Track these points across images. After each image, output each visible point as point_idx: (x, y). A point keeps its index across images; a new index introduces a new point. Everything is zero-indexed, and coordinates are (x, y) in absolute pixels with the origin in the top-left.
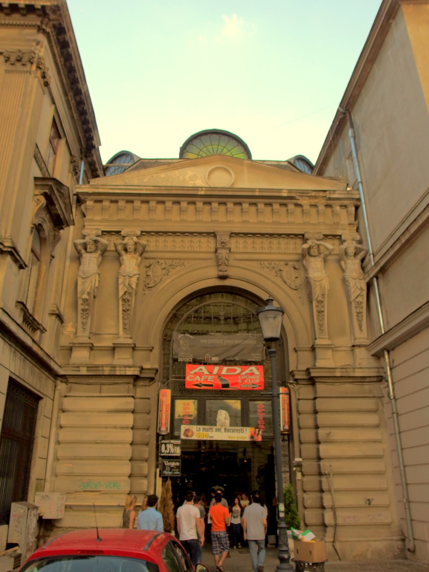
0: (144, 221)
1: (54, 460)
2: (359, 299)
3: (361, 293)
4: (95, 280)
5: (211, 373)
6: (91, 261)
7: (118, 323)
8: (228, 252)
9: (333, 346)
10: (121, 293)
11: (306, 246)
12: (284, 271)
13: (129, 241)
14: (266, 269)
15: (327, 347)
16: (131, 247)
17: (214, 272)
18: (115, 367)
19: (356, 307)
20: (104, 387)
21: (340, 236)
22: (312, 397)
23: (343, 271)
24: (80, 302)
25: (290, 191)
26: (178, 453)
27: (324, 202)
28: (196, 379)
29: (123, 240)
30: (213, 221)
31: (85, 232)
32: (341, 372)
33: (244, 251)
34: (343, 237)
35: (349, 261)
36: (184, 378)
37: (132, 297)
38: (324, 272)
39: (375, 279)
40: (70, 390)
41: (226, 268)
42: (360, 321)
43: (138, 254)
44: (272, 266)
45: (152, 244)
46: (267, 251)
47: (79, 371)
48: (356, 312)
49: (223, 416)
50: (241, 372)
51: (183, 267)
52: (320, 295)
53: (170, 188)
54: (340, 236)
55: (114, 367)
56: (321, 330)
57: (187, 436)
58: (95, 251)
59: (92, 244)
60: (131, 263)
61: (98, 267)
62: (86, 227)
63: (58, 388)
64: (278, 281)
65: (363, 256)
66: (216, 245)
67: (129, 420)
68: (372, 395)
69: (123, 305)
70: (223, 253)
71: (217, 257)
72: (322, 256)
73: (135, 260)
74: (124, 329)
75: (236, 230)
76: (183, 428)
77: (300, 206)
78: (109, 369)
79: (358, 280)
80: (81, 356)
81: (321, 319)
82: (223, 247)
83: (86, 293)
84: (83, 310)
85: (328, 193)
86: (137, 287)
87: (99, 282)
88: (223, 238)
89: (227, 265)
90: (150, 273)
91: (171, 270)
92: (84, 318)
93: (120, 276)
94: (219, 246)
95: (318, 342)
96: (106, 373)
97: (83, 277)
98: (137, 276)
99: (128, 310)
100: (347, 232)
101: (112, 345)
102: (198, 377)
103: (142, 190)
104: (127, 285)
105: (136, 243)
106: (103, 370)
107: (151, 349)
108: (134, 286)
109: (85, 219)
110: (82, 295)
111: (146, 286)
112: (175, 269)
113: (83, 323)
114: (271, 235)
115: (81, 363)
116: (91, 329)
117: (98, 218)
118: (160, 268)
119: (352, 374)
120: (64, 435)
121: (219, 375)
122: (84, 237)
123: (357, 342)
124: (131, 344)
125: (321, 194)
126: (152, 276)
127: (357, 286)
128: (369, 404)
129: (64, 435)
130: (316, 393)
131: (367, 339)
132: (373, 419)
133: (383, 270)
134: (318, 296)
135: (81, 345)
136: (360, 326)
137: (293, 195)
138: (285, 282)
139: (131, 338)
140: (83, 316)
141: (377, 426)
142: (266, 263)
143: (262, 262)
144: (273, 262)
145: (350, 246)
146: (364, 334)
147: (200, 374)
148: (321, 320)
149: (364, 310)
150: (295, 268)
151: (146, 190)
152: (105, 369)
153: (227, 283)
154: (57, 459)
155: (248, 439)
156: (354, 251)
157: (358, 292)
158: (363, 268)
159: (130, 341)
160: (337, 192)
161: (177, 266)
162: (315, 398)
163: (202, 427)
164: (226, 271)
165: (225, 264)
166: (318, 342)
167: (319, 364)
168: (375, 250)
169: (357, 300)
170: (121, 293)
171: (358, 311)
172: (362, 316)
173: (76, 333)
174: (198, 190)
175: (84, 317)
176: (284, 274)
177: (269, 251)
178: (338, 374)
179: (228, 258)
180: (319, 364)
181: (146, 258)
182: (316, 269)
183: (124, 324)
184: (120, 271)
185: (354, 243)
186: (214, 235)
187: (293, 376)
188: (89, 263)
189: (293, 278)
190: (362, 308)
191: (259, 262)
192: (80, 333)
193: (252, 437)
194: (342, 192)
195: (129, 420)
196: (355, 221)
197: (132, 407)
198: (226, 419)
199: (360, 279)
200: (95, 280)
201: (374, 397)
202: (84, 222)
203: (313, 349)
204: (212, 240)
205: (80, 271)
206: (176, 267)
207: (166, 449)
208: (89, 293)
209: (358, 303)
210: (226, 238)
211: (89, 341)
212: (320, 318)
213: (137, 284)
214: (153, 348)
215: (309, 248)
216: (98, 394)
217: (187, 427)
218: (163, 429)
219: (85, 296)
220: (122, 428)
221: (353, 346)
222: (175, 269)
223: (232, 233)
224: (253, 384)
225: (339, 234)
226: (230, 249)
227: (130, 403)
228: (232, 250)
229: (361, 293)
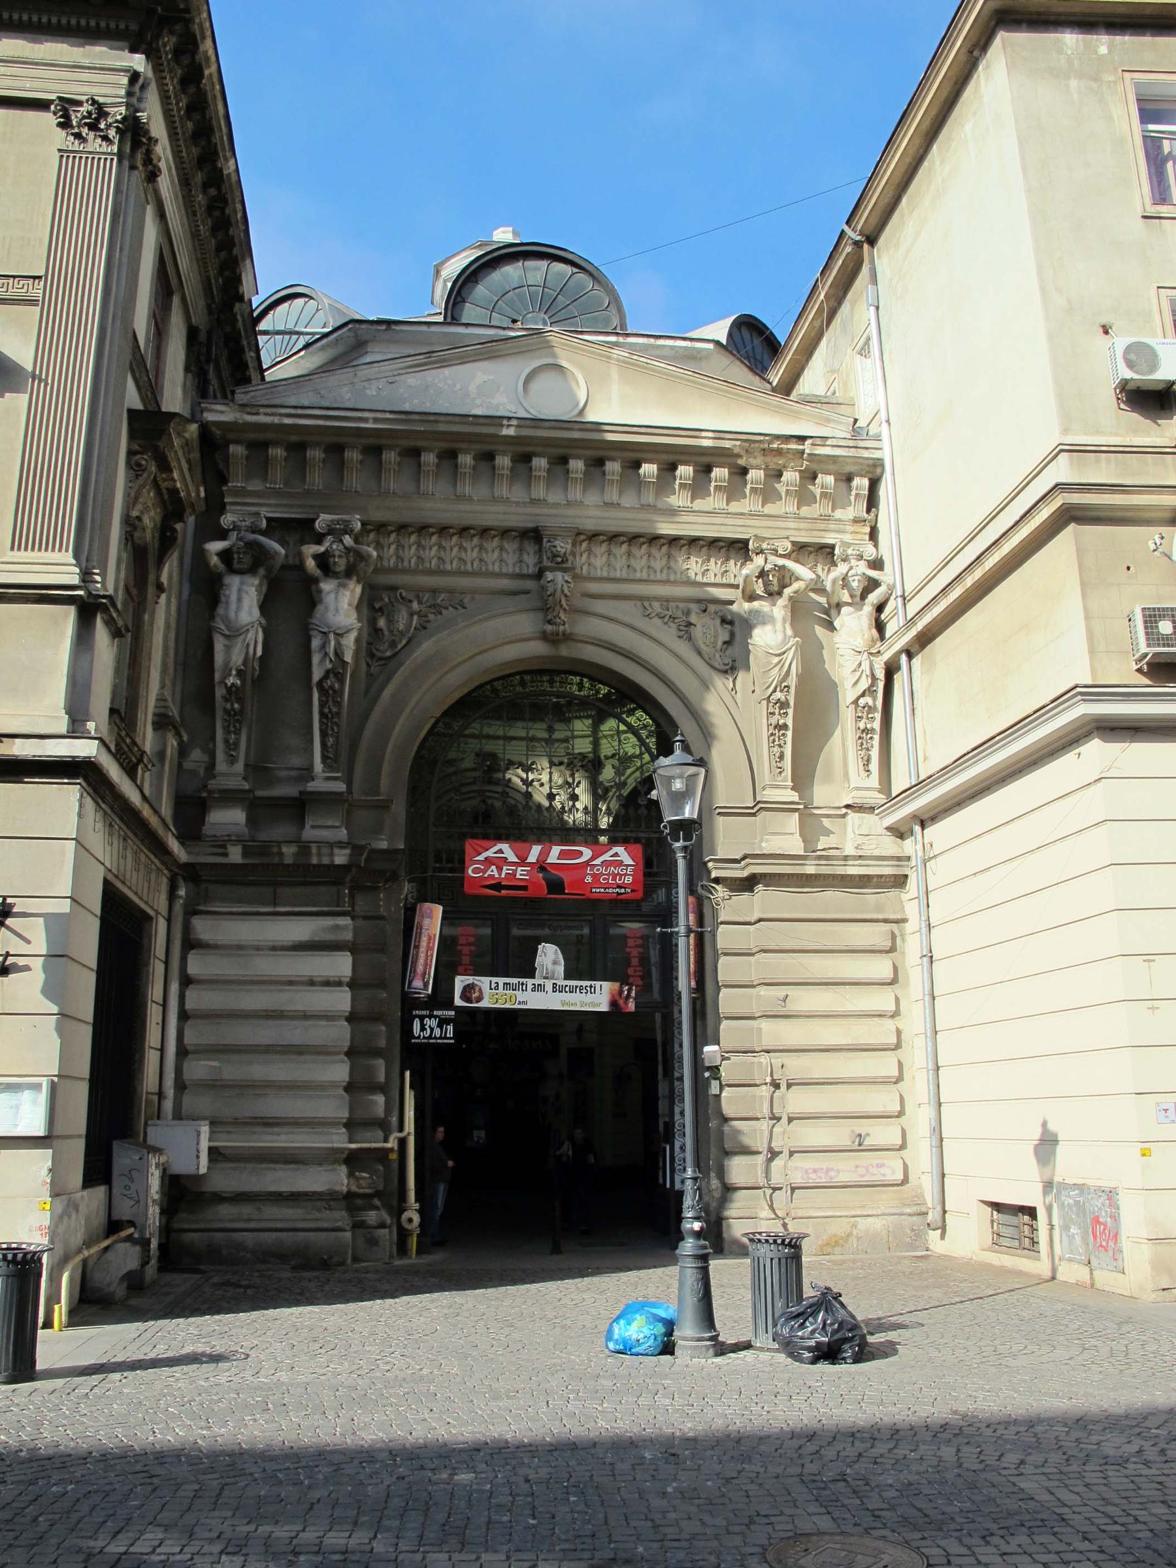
2: (868, 700)
3: (872, 685)
5: (523, 861)
10: (317, 675)
12: (699, 627)
14: (656, 621)
20: (284, 891)
24: (220, 692)
25: (719, 434)
26: (450, 1038)
28: (489, 872)
36: (463, 869)
37: (342, 682)
39: (904, 658)
44: (670, 613)
46: (659, 577)
49: (549, 956)
50: (593, 858)
53: (432, 418)
54: (833, 547)
57: (469, 1000)
62: (228, 507)
63: (182, 892)
64: (683, 648)
71: (543, 588)
73: (348, 593)
74: (324, 758)
75: (590, 525)
76: (460, 982)
83: (234, 672)
85: (808, 442)
90: (382, 623)
93: (313, 633)
94: (546, 563)
96: (288, 860)
97: (227, 633)
102: (493, 867)
103: (365, 420)
104: (332, 655)
109: (225, 488)
112: (441, 613)
113: (226, 741)
119: (840, 871)
120: (196, 999)
121: (541, 866)
125: (793, 446)
126: (386, 633)
128: (874, 935)
129: (196, 999)
132: (881, 968)
133: (925, 639)
137: (727, 444)
138: (700, 653)
140: (229, 726)
144: (672, 604)
146: (874, 781)
147: (501, 862)
151: (376, 420)
152: (284, 849)
153: (564, 651)
154: (183, 1052)
155: (604, 1007)
157: (864, 684)
158: (880, 627)
159: (341, 787)
161: (446, 608)
163: (502, 981)
168: (909, 589)
169: (862, 702)
170: (317, 675)
171: (862, 725)
174: (502, 426)
176: (697, 632)
177: (664, 576)
183: (324, 744)
184: (314, 621)
185: (862, 564)
189: (720, 643)
191: (639, 603)
192: (221, 766)
193: (614, 1003)
196: (868, 511)
197: (348, 936)
198: (555, 963)
199: (871, 654)
200: (256, 642)
204: (530, 548)
205: (218, 619)
206: (444, 611)
207: (423, 1029)
208: (240, 673)
210: (563, 546)
216: (271, 909)
217: (470, 979)
218: (418, 983)
220: (327, 983)
224: (619, 887)
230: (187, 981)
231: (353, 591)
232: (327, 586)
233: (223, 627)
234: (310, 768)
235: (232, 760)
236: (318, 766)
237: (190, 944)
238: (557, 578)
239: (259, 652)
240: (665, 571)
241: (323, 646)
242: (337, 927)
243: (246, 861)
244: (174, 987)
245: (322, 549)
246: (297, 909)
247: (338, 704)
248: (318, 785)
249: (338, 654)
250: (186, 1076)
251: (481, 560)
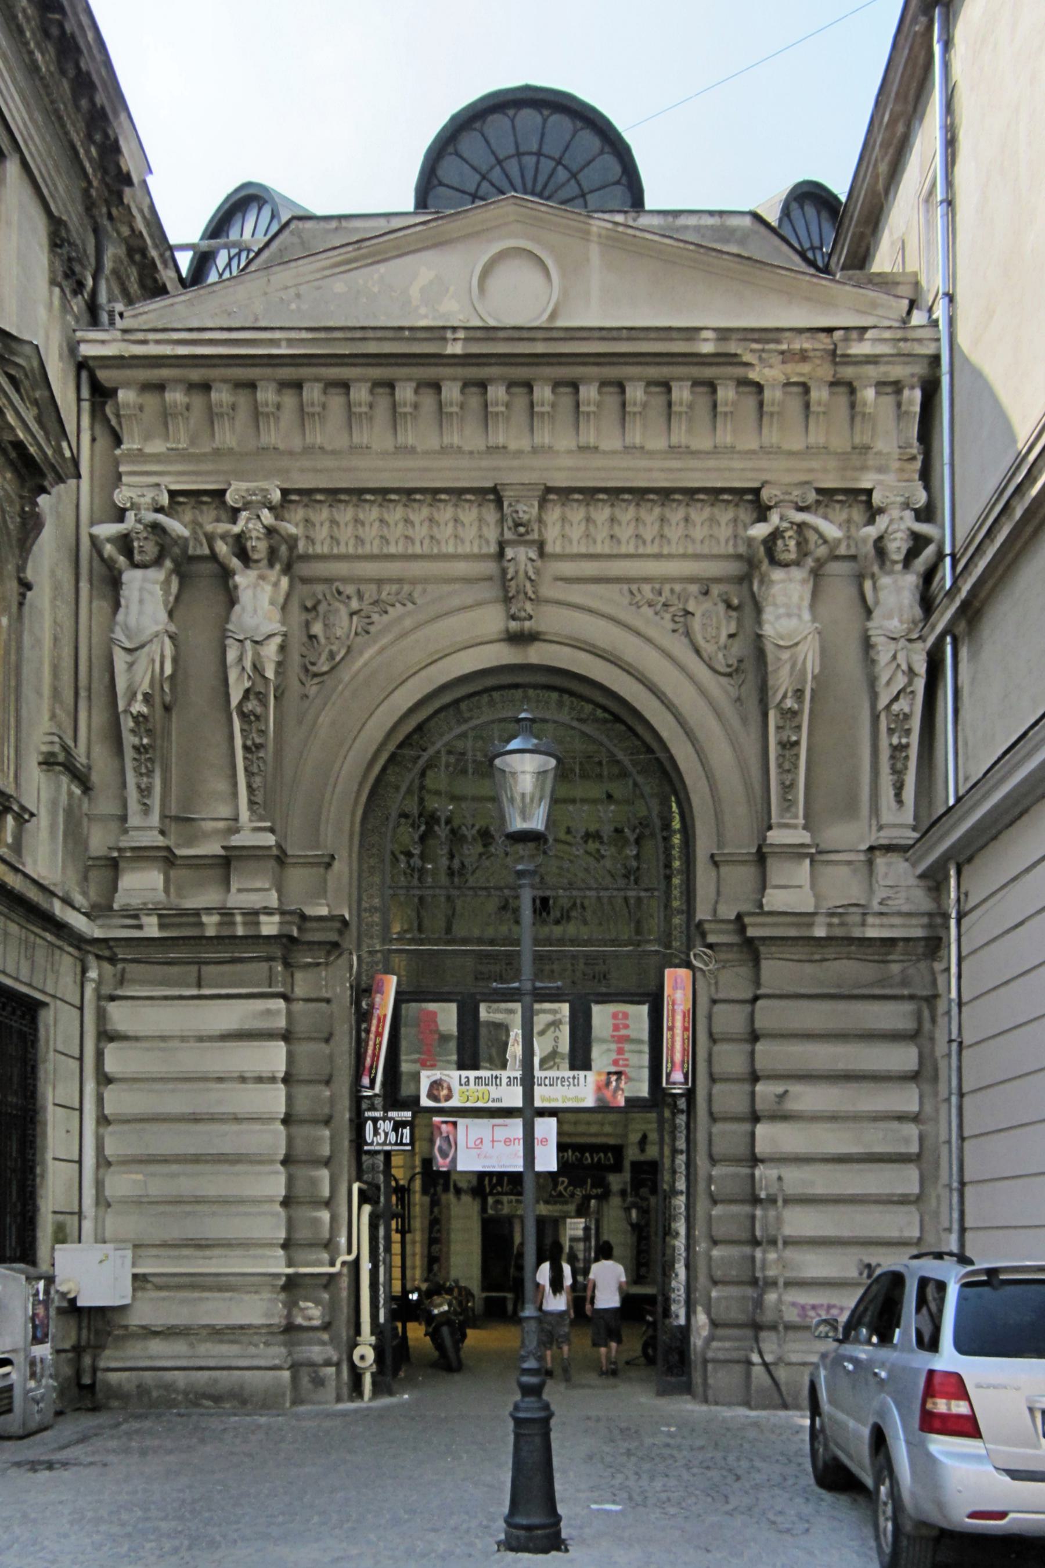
0: (291, 453)
1: (98, 1166)
4: (162, 657)
6: (147, 594)
7: (235, 785)
8: (533, 555)
9: (813, 851)
10: (234, 701)
11: (760, 531)
12: (698, 615)
13: (250, 526)
15: (795, 853)
16: (259, 547)
17: (492, 620)
18: (232, 914)
19: (891, 731)
20: (208, 970)
21: (869, 492)
22: (749, 995)
23: (869, 612)
27: (826, 372)
29: (234, 521)
30: (493, 450)
31: (121, 496)
32: (830, 925)
33: (583, 550)
34: (877, 499)
35: (885, 581)
37: (265, 705)
38: (807, 616)
40: (122, 980)
41: (529, 607)
42: (898, 773)
43: (278, 567)
45: (319, 531)
47: (140, 927)
48: (891, 745)
51: (410, 606)
52: (790, 694)
54: (869, 492)
55: (226, 914)
56: (786, 800)
58: (158, 562)
59: (146, 538)
60: (260, 601)
61: (171, 614)
62: (125, 479)
63: (93, 974)
65: (932, 560)
66: (502, 534)
67: (274, 1057)
68: (906, 992)
69: (242, 730)
70: (520, 555)
72: (810, 562)
73: (268, 588)
75: (561, 480)
77: (759, 388)
78: (215, 919)
79: (902, 642)
80: (142, 884)
81: (788, 768)
82: (521, 541)
83: (140, 697)
84: (136, 748)
86: (277, 673)
87: (175, 661)
88: (521, 507)
89: (531, 599)
91: (375, 617)
92: (141, 775)
93: (229, 641)
94: (508, 535)
95: (775, 837)
96: (211, 932)
97: (128, 645)
98: (278, 640)
99: (259, 747)
100: (890, 478)
101: (222, 852)
105: (270, 531)
106: (201, 925)
107: (326, 860)
108: (270, 674)
109: (118, 452)
110: (129, 705)
111: (307, 670)
114: (666, 494)
115: (145, 904)
116: (163, 805)
117: (156, 446)
118: (344, 612)
120: (116, 1101)
122: (120, 515)
123: (884, 837)
124: (269, 848)
127: (900, 662)
129: (116, 1101)
130: (757, 983)
131: (914, 829)
132: (904, 1058)
134: (784, 697)
135: (142, 855)
136: (899, 788)
138: (698, 652)
139: (272, 830)
140: (139, 766)
141: (914, 1077)
142: (646, 588)
143: (634, 587)
144: (667, 588)
145: (897, 526)
148: (789, 771)
149: (914, 739)
150: (729, 606)
152: (205, 919)
154: (103, 1162)
156: (905, 547)
159: (270, 840)
160: (869, 335)
162: (756, 998)
164: (531, 617)
165: (526, 594)
166: (775, 837)
167: (775, 899)
169: (895, 707)
171: (895, 741)
172: (907, 757)
173: (124, 818)
175: (144, 770)
176: (696, 624)
178: (820, 932)
179: (533, 577)
180: (775, 899)
181: (305, 581)
182: (789, 610)
184: (230, 627)
185: (909, 515)
186: (493, 495)
187: (704, 935)
188: (141, 601)
190: (908, 732)
192: (134, 820)
194: (887, 334)
195: (274, 1057)
197: (282, 1023)
201: (912, 997)
202: (117, 463)
203: (761, 858)
205: (118, 629)
208: (147, 698)
209: (897, 715)
210: (528, 510)
211: (160, 841)
212: (787, 766)
213: (279, 664)
214: (333, 857)
215: (776, 535)
216: (194, 992)
219: (139, 707)
220: (260, 1080)
221: (871, 849)
222: (386, 612)
223: (549, 490)
225: (866, 485)
226: (541, 545)
227: (274, 1012)
228: (549, 549)
229: (910, 683)
230: (105, 1079)
231: (276, 585)
232: (243, 579)
233: (122, 638)
234: (236, 819)
235: (146, 809)
236: (244, 814)
237: (106, 1036)
238: (520, 555)
239: (168, 670)
240: (657, 541)
241: (240, 659)
242: (268, 1012)
243: (165, 934)
244: (90, 1087)
245: (236, 529)
246: (223, 991)
247: (263, 732)
248: (244, 839)
249: (258, 669)
250: (108, 1192)
251: (432, 537)
